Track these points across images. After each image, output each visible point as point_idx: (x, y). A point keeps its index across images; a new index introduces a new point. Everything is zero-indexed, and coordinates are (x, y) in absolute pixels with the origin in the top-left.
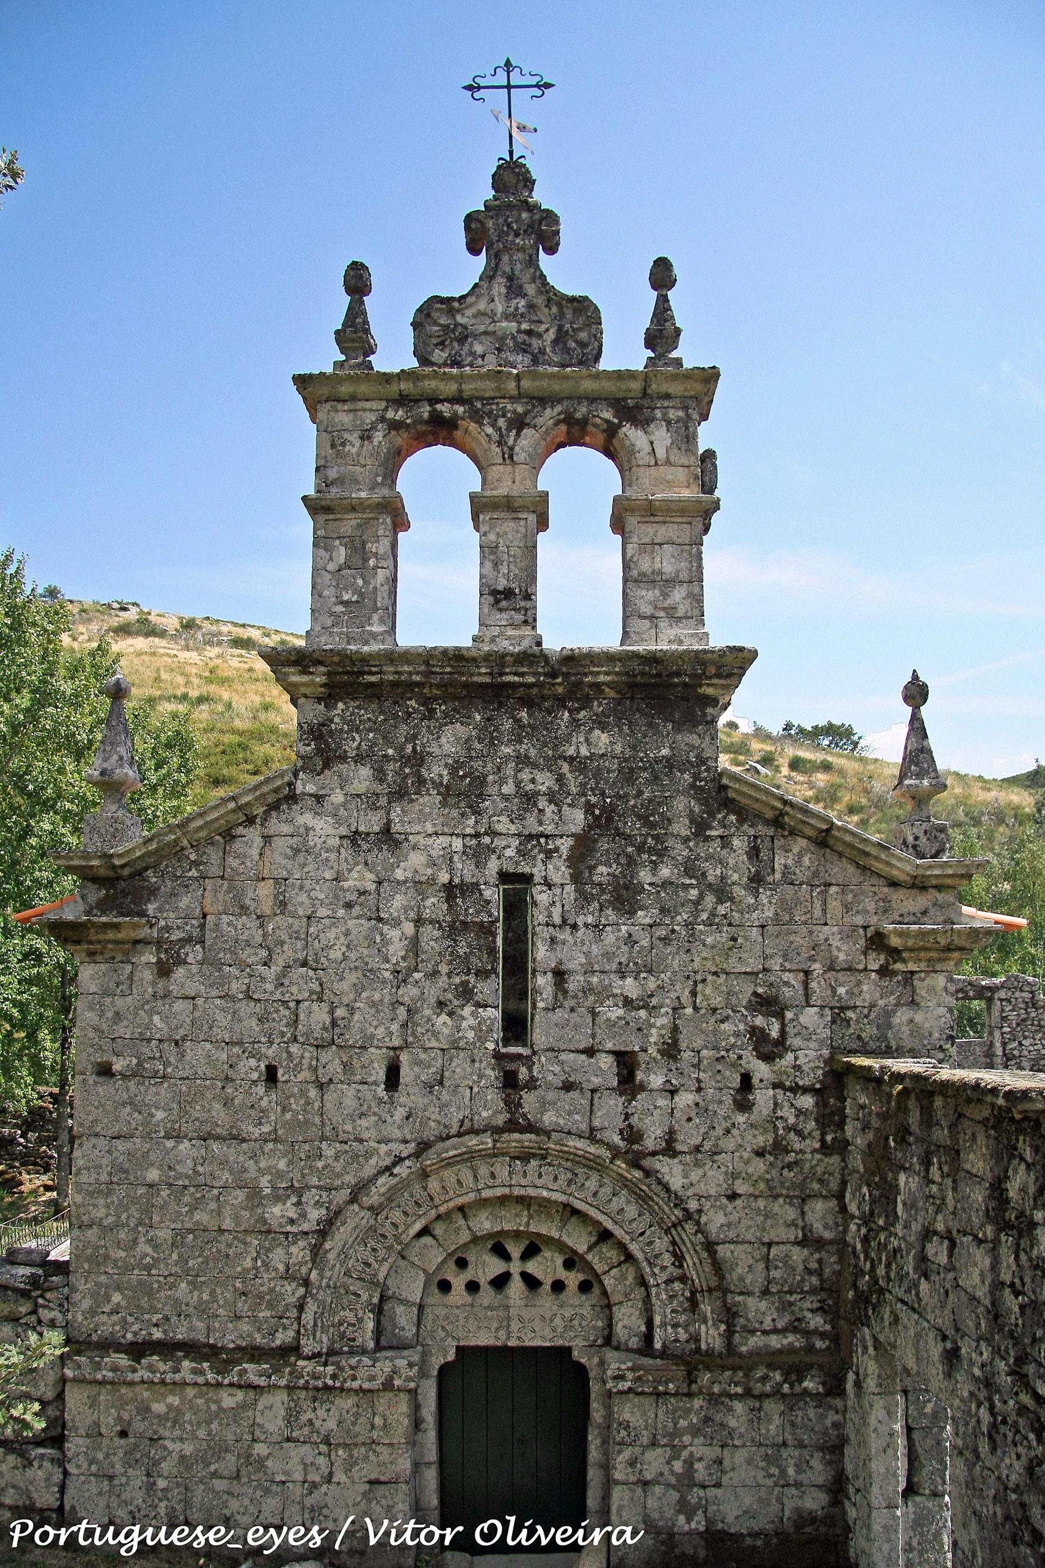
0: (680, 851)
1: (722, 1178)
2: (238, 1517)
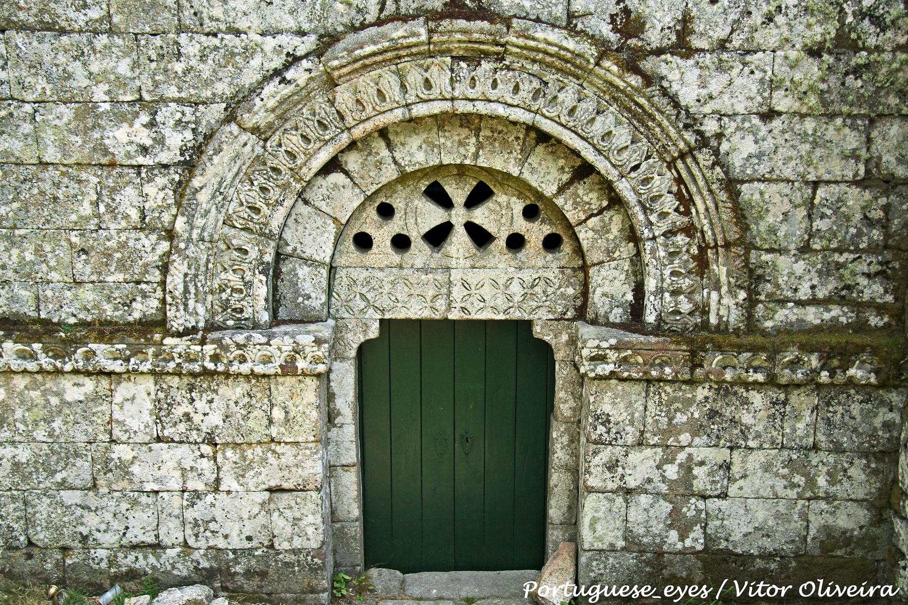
1: (754, 88)
2: (98, 535)
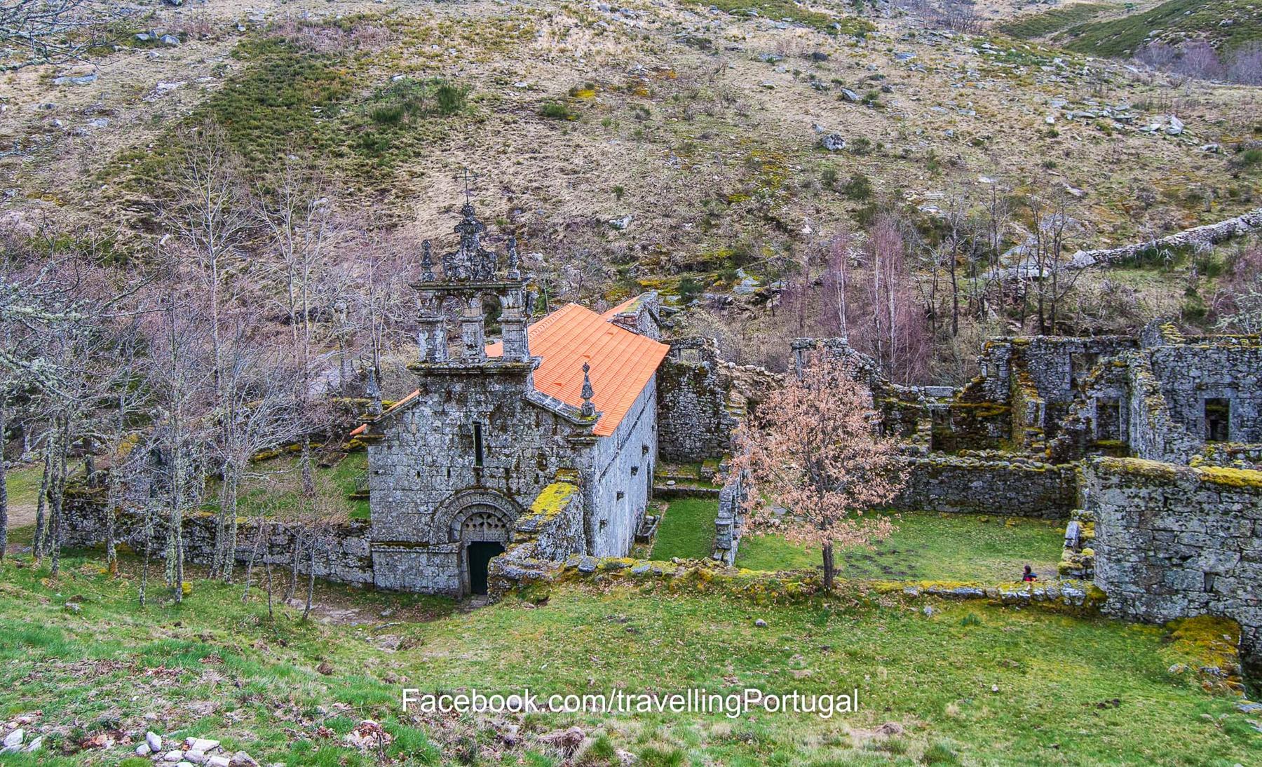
0: (519, 416)
